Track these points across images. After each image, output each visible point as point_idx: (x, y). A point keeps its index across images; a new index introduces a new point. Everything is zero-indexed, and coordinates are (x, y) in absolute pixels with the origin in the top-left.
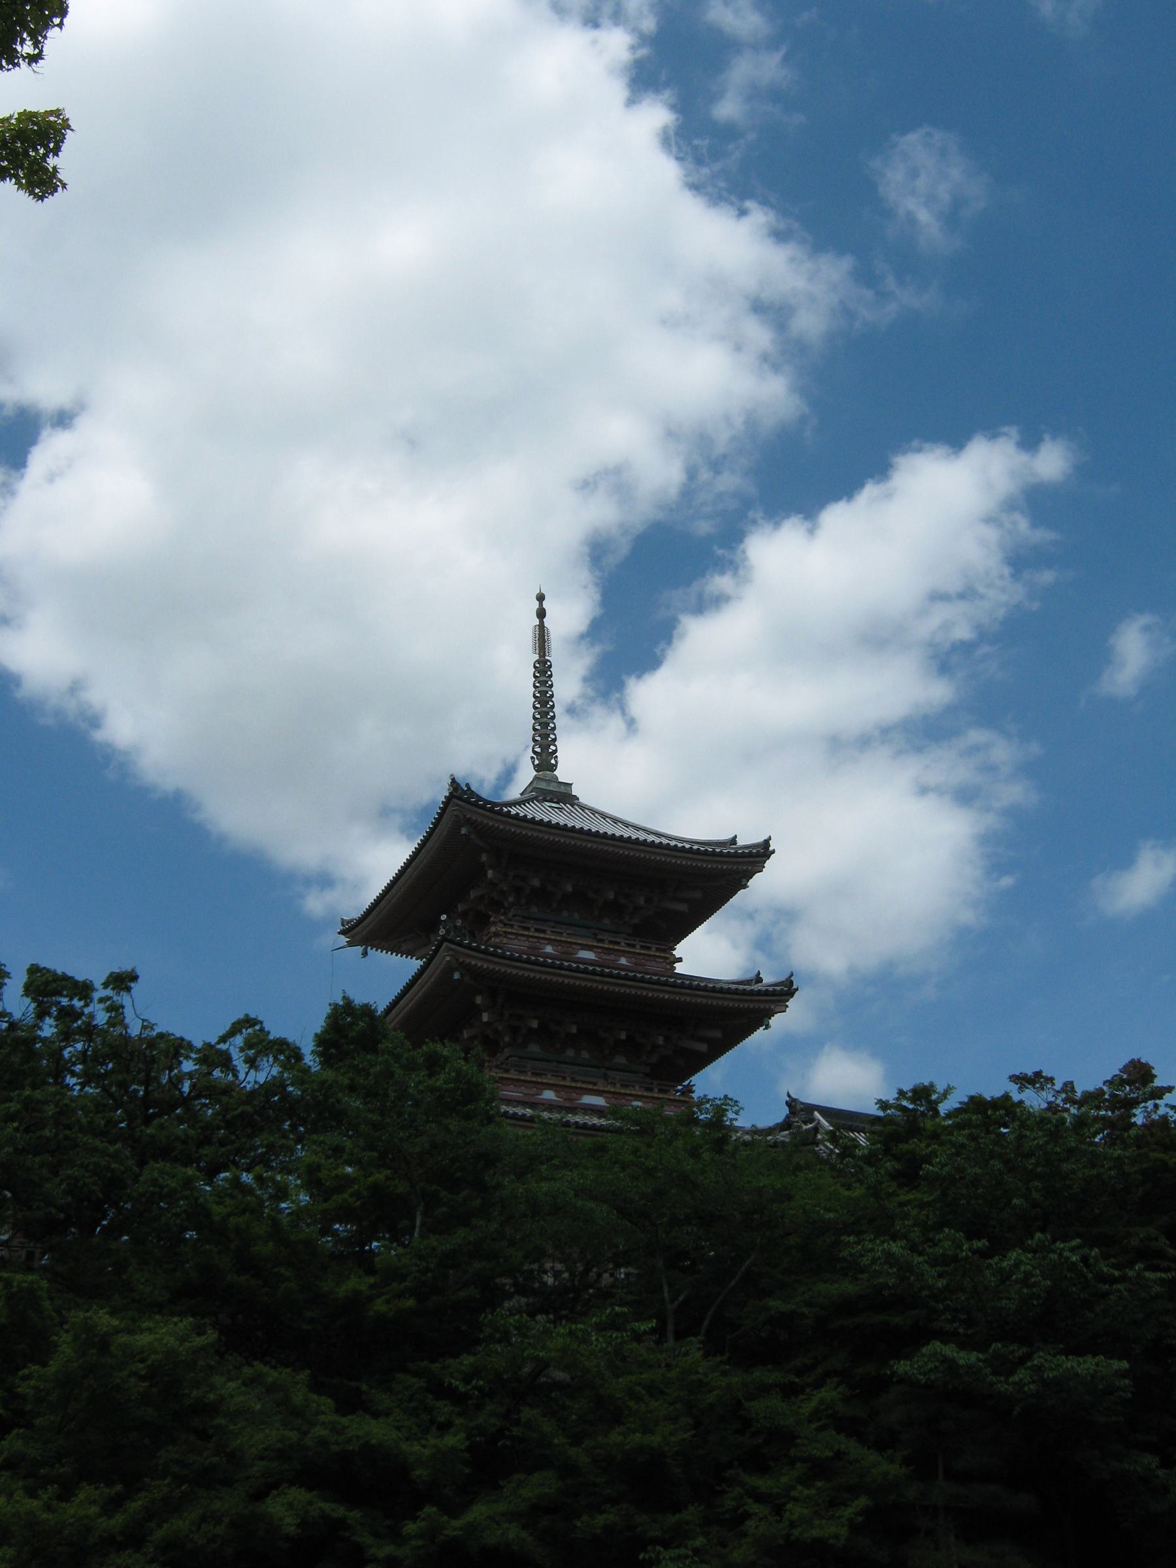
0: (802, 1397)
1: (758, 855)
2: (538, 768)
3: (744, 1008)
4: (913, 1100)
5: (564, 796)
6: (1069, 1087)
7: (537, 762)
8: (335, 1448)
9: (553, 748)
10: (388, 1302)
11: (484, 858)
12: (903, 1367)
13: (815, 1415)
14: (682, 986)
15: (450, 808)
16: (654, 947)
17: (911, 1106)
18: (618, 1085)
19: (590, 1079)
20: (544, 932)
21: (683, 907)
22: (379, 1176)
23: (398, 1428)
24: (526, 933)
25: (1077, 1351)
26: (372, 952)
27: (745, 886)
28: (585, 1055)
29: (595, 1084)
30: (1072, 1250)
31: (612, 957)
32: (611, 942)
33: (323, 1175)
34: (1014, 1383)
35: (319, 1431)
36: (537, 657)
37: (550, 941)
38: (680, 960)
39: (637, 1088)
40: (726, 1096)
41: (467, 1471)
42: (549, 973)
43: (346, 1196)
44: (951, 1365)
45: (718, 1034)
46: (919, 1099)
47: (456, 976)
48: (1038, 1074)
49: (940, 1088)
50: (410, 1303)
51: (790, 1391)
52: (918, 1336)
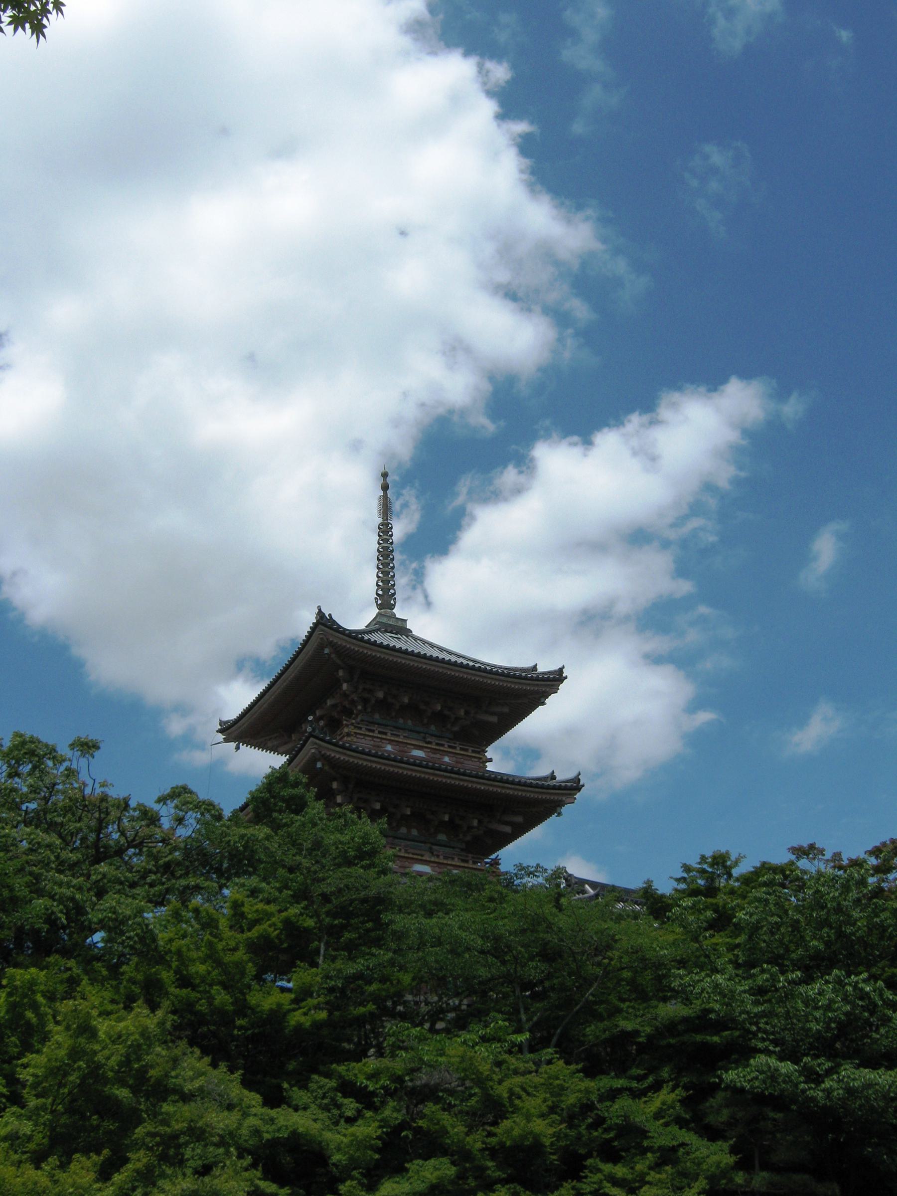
0: (644, 1099)
1: (554, 680)
2: (380, 607)
3: (540, 800)
4: (712, 865)
5: (401, 629)
6: (837, 856)
7: (379, 602)
8: (267, 1136)
9: (392, 591)
10: (305, 1014)
11: (341, 673)
13: (658, 1116)
14: (495, 780)
15: (316, 633)
16: (470, 749)
17: (710, 870)
18: (441, 857)
19: (418, 852)
20: (385, 734)
21: (494, 719)
22: (294, 911)
23: (315, 1120)
24: (371, 734)
25: (873, 1064)
26: (243, 747)
27: (543, 704)
28: (415, 832)
29: (422, 856)
31: (438, 756)
32: (437, 744)
33: (246, 909)
34: (823, 1091)
35: (252, 1121)
36: (380, 520)
37: (391, 742)
38: (490, 760)
39: (456, 859)
40: (538, 865)
41: (377, 1156)
44: (774, 1075)
45: (519, 819)
46: (717, 864)
47: (319, 765)
48: (812, 847)
49: (733, 858)
50: (323, 1015)
51: (636, 1094)
52: (740, 1052)
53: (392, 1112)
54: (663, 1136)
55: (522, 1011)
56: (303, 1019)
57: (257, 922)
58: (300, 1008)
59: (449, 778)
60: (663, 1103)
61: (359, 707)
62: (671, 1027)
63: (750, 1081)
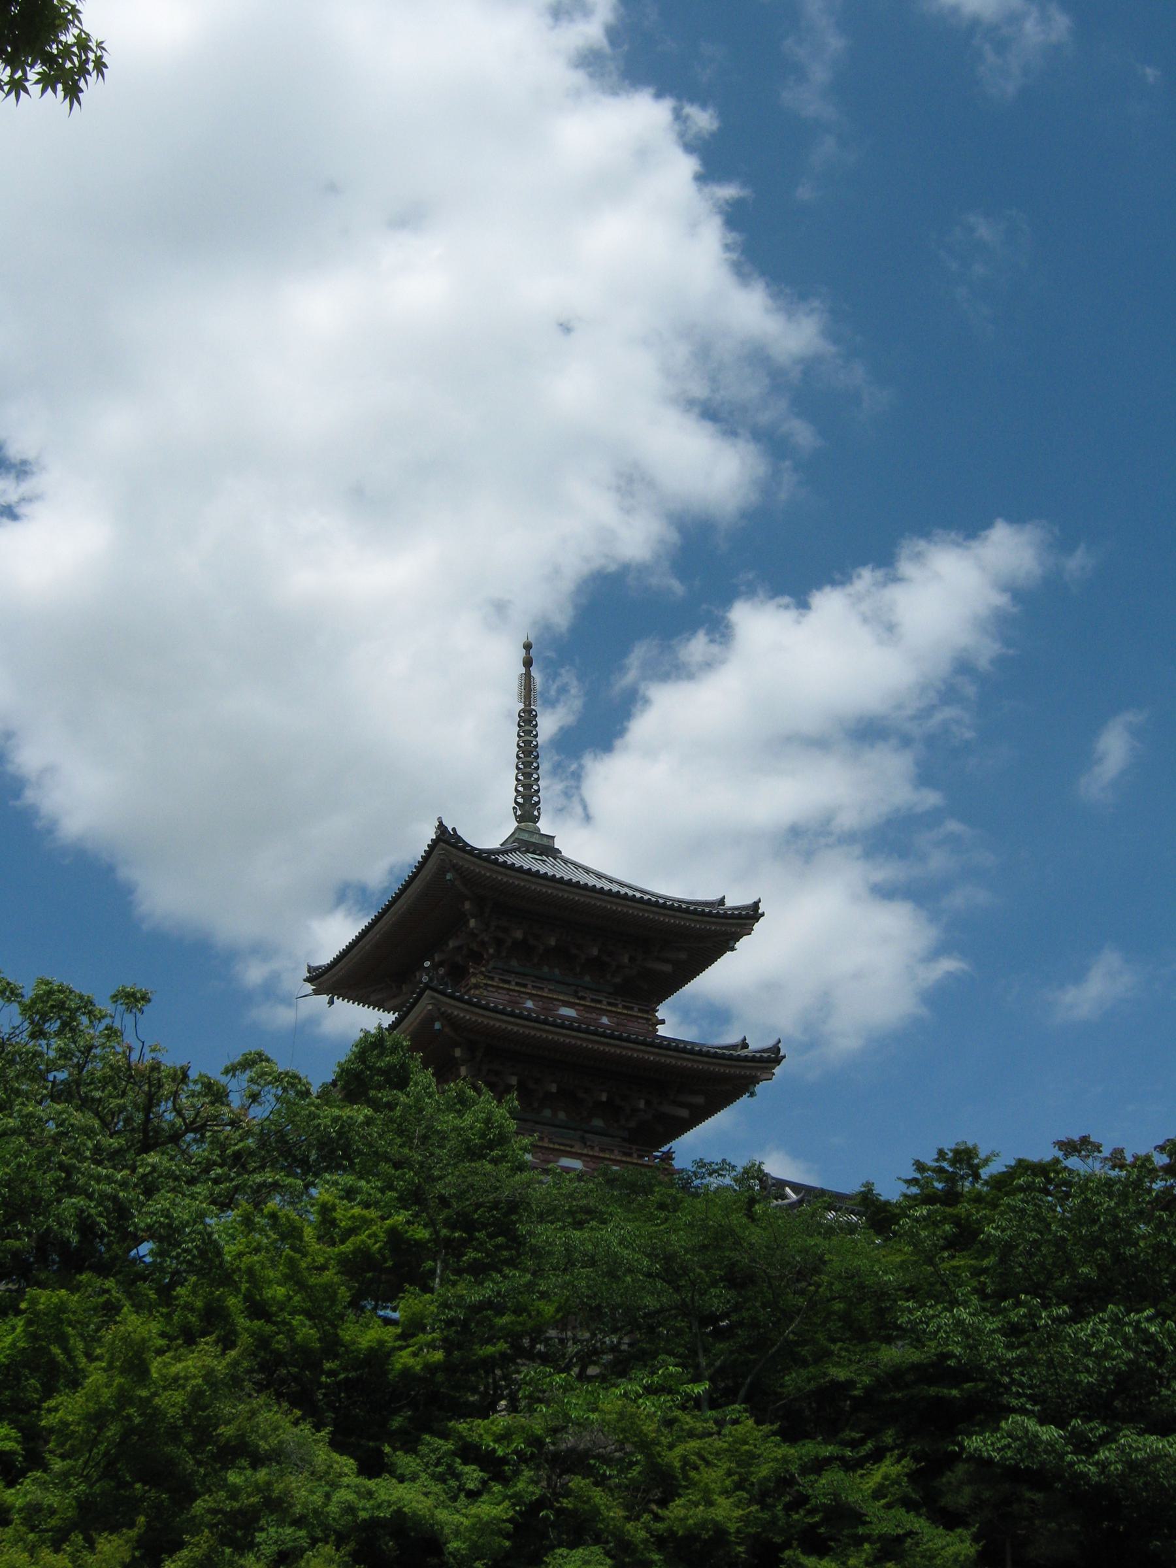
1: (748, 917)
2: (520, 819)
3: (728, 1075)
4: (953, 1163)
5: (547, 849)
6: (1118, 1153)
7: (519, 813)
8: (363, 1515)
9: (536, 799)
10: (415, 1355)
11: (467, 905)
12: (974, 1443)
13: (878, 1494)
14: (668, 1048)
17: (951, 1170)
18: (597, 1149)
19: (569, 1142)
20: (525, 986)
21: (668, 968)
22: (400, 1218)
23: (426, 1494)
24: (506, 986)
26: (338, 1002)
27: (733, 949)
28: (562, 1115)
29: (572, 1147)
30: (1149, 1319)
31: (594, 1016)
32: (593, 1000)
33: (338, 1214)
34: (1096, 1464)
35: (343, 1495)
36: (522, 706)
37: (532, 996)
38: (663, 1022)
39: (616, 1152)
40: (724, 1161)
41: (507, 1543)
42: (534, 1028)
43: (363, 1237)
44: (1032, 1443)
45: (700, 1100)
46: (960, 1161)
47: (437, 1026)
48: (1085, 1140)
49: (982, 1155)
50: (439, 1356)
51: (849, 1466)
52: (988, 1410)
53: (527, 1484)
54: (886, 1521)
55: (700, 1352)
56: (411, 1361)
57: (351, 1231)
58: (408, 1346)
59: (608, 1044)
60: (886, 1477)
61: (491, 951)
62: (896, 1376)
63: (1000, 1450)
